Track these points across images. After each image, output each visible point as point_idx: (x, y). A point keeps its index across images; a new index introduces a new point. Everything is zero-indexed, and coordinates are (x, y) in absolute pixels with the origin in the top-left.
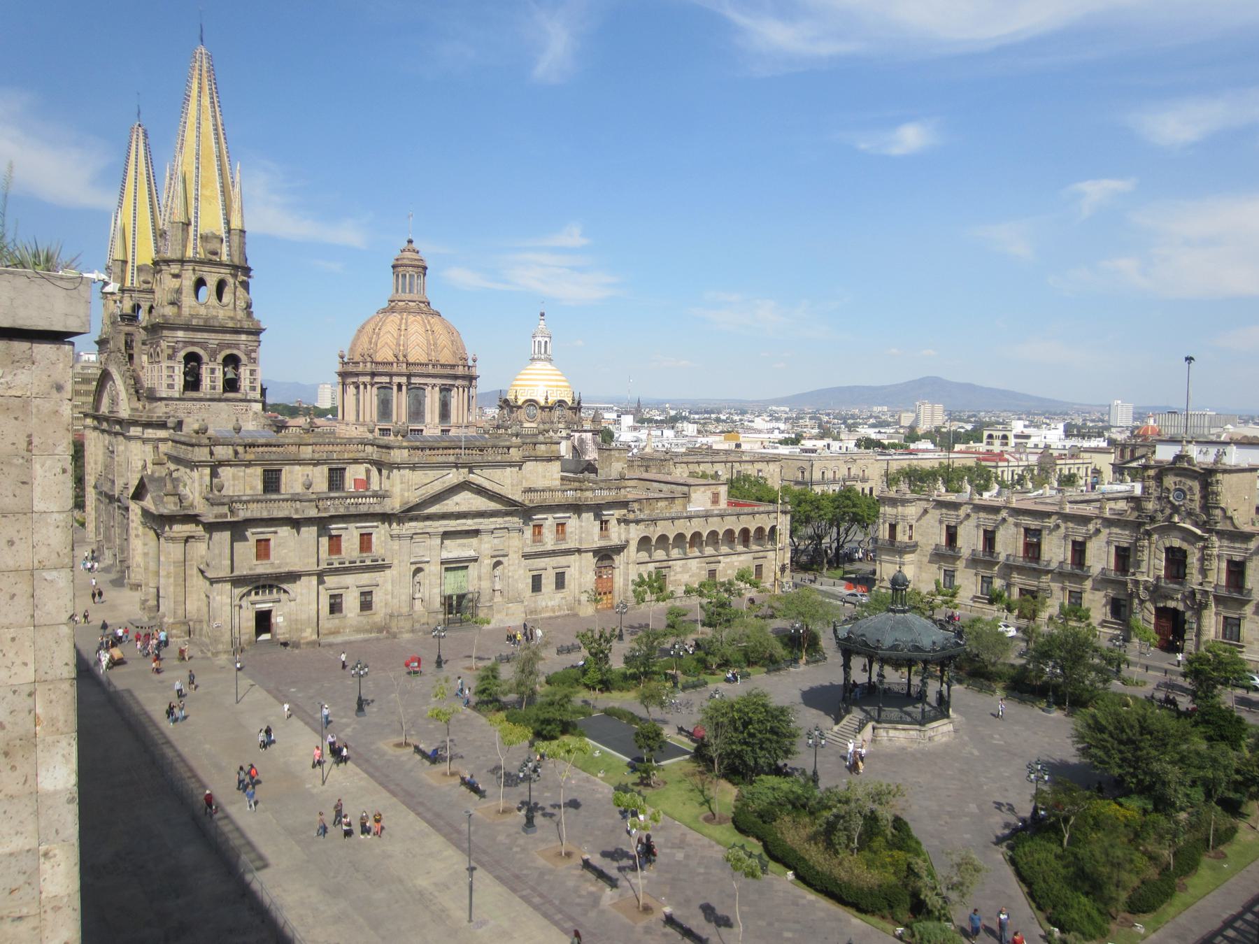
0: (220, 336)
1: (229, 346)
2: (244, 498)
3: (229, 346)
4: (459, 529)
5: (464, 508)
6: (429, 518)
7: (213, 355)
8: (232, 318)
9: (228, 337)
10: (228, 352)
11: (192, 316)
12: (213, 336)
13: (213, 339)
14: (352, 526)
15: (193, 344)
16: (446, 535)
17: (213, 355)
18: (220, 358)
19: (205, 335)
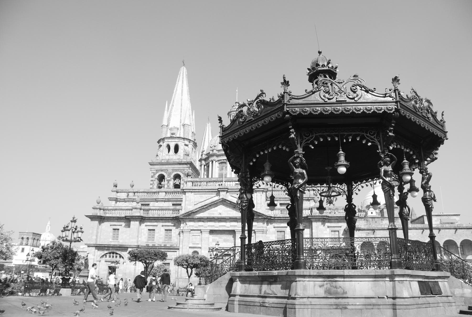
0: (173, 166)
1: (176, 170)
2: (110, 208)
3: (176, 170)
4: (221, 229)
5: (224, 215)
6: (201, 220)
7: (169, 175)
8: (178, 159)
9: (176, 166)
10: (176, 173)
11: (162, 160)
12: (170, 166)
13: (170, 167)
14: (160, 224)
15: (162, 170)
16: (212, 232)
17: (169, 175)
18: (172, 176)
19: (167, 166)
